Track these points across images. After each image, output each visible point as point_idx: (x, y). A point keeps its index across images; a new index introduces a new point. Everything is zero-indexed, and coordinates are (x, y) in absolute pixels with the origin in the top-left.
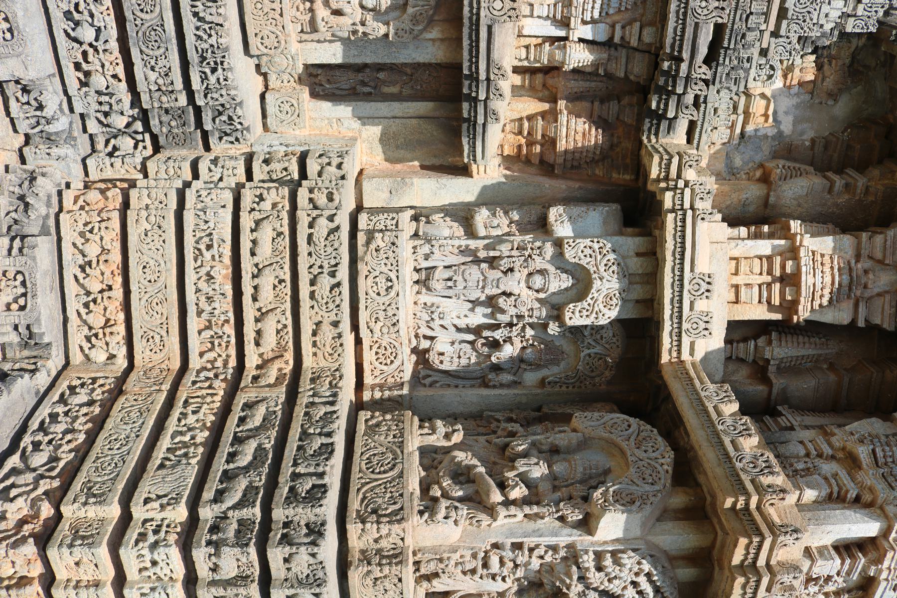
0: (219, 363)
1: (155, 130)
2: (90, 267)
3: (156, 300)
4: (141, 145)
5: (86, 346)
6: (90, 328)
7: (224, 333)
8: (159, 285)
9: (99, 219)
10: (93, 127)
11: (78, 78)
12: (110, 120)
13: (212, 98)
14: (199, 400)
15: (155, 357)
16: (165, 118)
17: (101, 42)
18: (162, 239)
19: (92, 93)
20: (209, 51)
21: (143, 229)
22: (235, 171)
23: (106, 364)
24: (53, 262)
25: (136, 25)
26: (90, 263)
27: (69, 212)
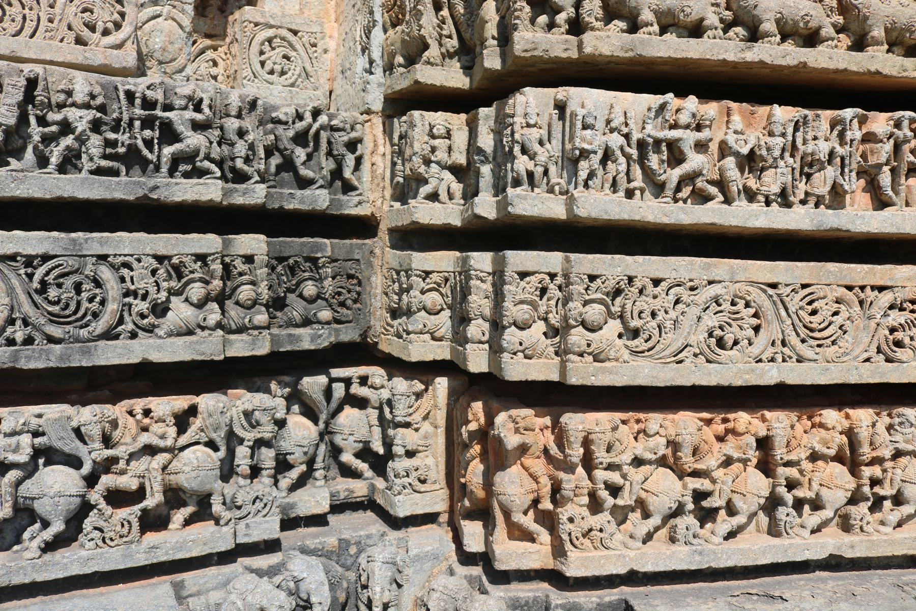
3: (808, 318)
4: (357, 389)
6: (853, 500)
7: (891, 136)
8: (767, 304)
9: (580, 470)
10: (313, 499)
11: (188, 522)
12: (297, 456)
13: (247, 160)
16: (296, 308)
17: (82, 450)
18: (650, 286)
19: (229, 489)
20: (112, 136)
21: (619, 342)
22: (439, 130)
24: (697, 595)
25: (29, 341)
26: (699, 496)
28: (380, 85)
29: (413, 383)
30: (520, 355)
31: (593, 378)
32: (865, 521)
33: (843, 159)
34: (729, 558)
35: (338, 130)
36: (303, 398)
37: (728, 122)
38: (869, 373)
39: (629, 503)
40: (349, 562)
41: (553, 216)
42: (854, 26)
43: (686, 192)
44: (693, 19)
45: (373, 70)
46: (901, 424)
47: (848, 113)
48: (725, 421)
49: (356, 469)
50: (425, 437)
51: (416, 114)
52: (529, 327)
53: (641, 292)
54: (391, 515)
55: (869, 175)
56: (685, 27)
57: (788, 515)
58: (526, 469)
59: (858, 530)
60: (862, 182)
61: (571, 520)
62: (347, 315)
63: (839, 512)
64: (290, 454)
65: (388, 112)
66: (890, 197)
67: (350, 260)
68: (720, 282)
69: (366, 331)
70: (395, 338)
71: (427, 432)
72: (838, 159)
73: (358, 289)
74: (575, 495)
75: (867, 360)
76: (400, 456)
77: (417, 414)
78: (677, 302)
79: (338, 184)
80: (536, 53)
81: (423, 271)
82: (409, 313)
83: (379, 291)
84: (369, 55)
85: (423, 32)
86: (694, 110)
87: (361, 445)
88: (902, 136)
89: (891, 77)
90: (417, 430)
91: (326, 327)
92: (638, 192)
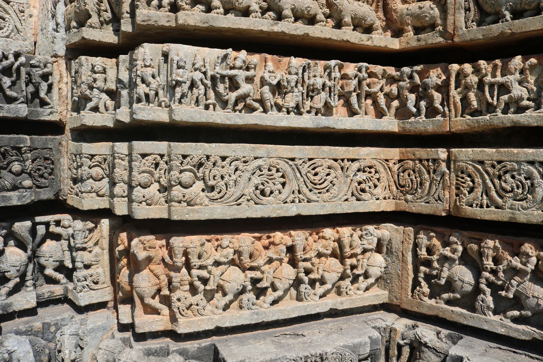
0: (394, 88)
1: (28, 197)
2: (259, 280)
3: (312, 178)
4: (53, 229)
5: (363, 283)
6: (343, 278)
8: (289, 170)
9: (184, 270)
10: (26, 299)
12: (12, 273)
14: (472, 96)
15: (384, 182)
21: (202, 194)
22: (98, 68)
23: (389, 252)
24: (255, 338)
26: (255, 281)
27: (173, 319)
28: (63, 39)
29: (87, 223)
30: (144, 203)
31: (187, 216)
32: (348, 289)
33: (330, 88)
34: (274, 315)
35: (35, 67)
36: (16, 235)
37: (265, 66)
38: (347, 207)
39: (213, 288)
40: (50, 337)
41: (161, 120)
42: (335, 15)
43: (240, 106)
44: (244, 6)
45: (58, 30)
46: (366, 234)
47: (333, 63)
48: (269, 237)
49: (55, 278)
50: (96, 256)
51: (83, 58)
52: (149, 187)
53: (214, 164)
54: (76, 305)
55: (345, 97)
56: (239, 11)
57: (306, 289)
58: (152, 271)
59: (345, 294)
60: (342, 101)
61: (179, 300)
62: (45, 183)
63: (336, 285)
64: (7, 272)
65: (69, 57)
66: (357, 110)
67: (46, 149)
68: (261, 158)
69: (58, 193)
70: (75, 196)
71: (97, 253)
72: (328, 88)
73: (51, 166)
74: (181, 285)
75: (346, 200)
76: (80, 268)
77: (90, 242)
78: (236, 170)
79: (37, 101)
80: (150, 23)
81: (90, 155)
82: (82, 180)
83: (66, 167)
84: (56, 20)
85: (87, 7)
86: (244, 59)
87: (58, 263)
88: (362, 76)
89: (355, 44)
90: (90, 252)
91: (28, 190)
92: (211, 106)
